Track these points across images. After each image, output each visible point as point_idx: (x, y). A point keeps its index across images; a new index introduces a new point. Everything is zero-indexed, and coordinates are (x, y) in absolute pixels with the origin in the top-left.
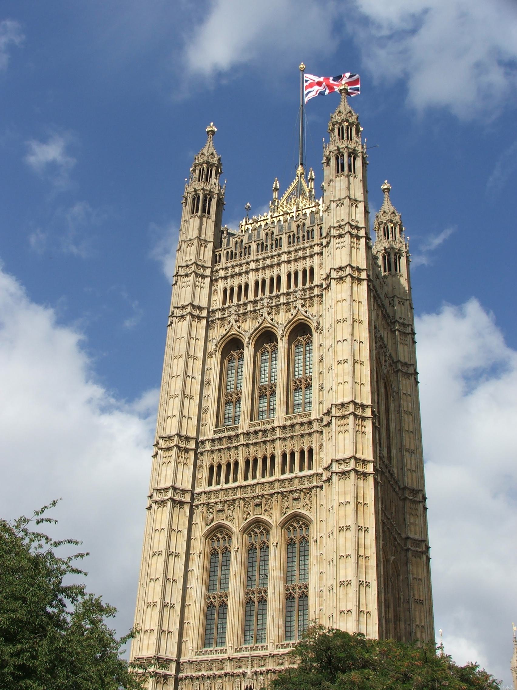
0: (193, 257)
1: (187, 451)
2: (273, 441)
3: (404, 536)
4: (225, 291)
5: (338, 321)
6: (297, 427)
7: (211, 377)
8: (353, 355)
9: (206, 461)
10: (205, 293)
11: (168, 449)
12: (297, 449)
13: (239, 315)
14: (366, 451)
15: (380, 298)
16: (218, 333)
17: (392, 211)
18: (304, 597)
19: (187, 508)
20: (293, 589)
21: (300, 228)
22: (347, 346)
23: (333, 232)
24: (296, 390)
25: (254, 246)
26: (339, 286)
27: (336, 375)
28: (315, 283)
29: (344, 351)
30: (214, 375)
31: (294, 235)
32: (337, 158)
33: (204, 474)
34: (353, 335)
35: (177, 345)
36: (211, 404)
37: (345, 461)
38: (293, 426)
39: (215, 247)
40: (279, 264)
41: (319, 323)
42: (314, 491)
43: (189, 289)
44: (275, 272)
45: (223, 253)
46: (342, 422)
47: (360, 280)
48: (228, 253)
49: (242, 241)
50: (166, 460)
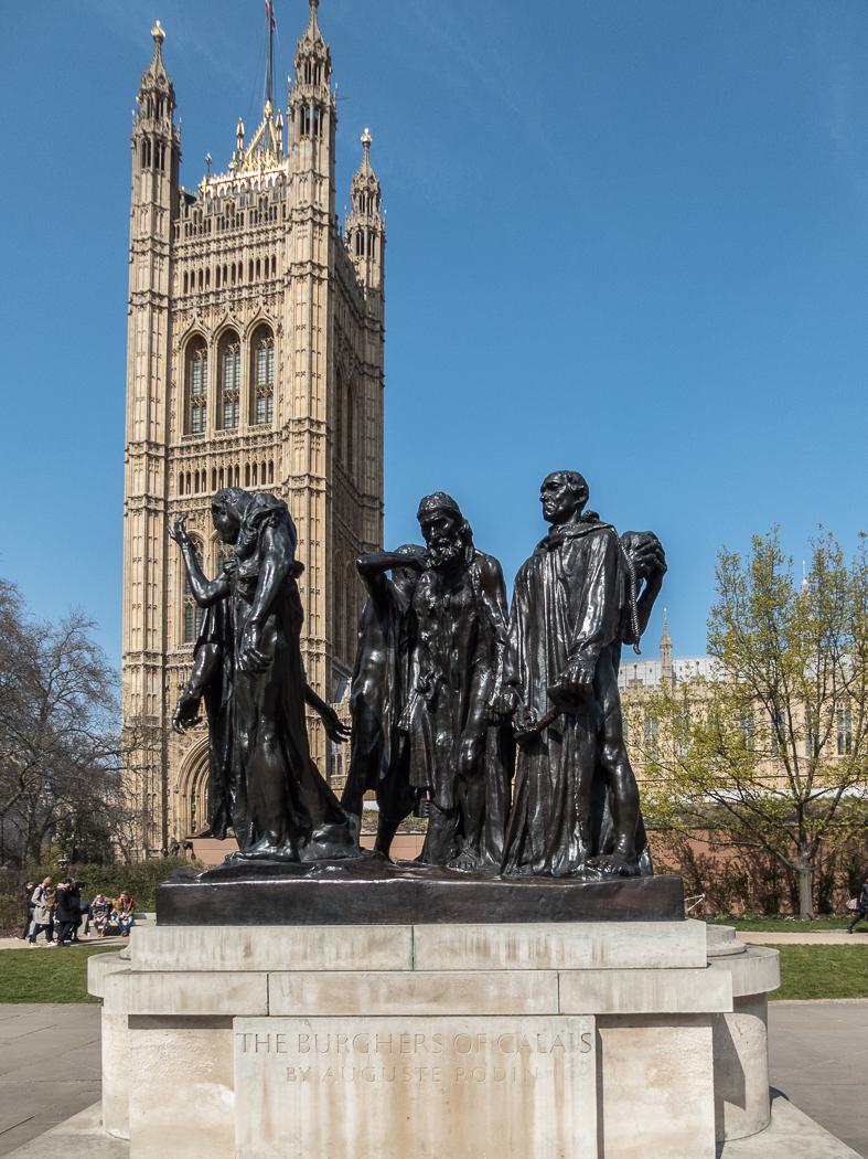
0: (149, 229)
1: (157, 458)
2: (237, 452)
3: (360, 541)
5: (298, 328)
6: (259, 439)
7: (177, 378)
8: (311, 368)
10: (165, 276)
11: (139, 456)
13: (201, 308)
14: (319, 469)
15: (348, 292)
16: (180, 327)
17: (370, 174)
19: (161, 516)
21: (263, 204)
22: (305, 358)
23: (296, 217)
24: (259, 398)
25: (214, 222)
26: (299, 285)
27: (294, 389)
28: (277, 278)
29: (302, 363)
30: (178, 376)
31: (256, 212)
33: (174, 483)
34: (311, 344)
35: (139, 339)
38: (255, 438)
41: (280, 326)
43: (147, 271)
45: (182, 226)
46: (298, 439)
47: (321, 280)
48: (187, 225)
49: (201, 212)
50: (137, 468)
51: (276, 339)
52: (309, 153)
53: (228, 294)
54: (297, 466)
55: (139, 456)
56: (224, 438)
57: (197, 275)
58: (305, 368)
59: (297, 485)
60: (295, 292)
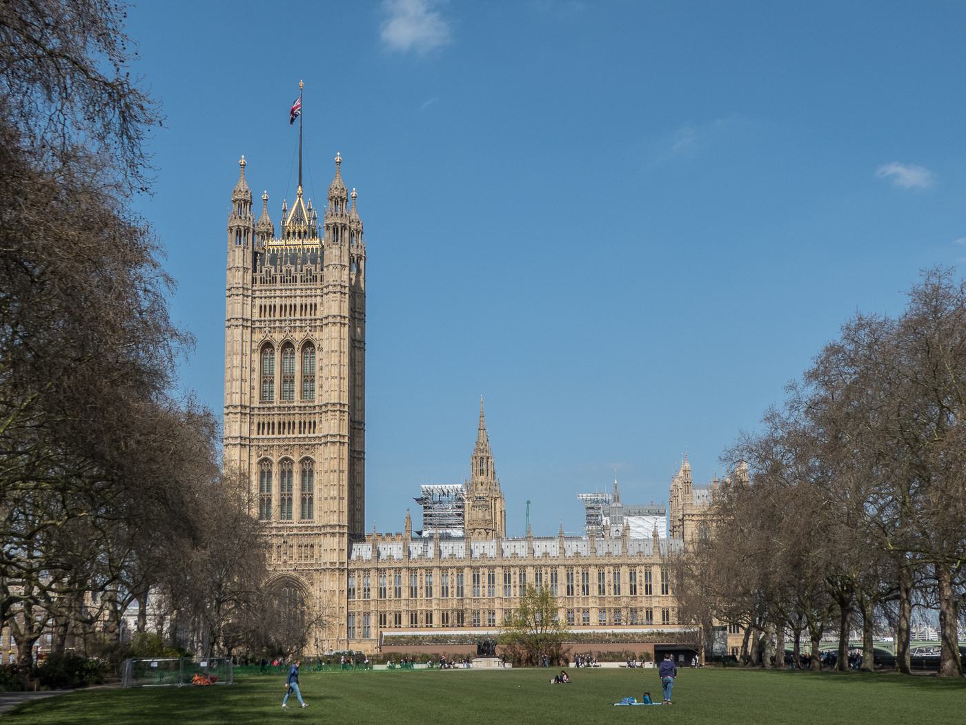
0: (240, 281)
1: (245, 414)
4: (261, 307)
8: (340, 375)
9: (256, 419)
11: (235, 414)
12: (307, 421)
16: (258, 337)
18: (311, 499)
20: (306, 495)
25: (278, 279)
26: (333, 328)
29: (335, 371)
30: (257, 366)
32: (334, 229)
33: (255, 427)
34: (340, 362)
35: (235, 345)
36: (256, 384)
37: (334, 436)
38: (305, 407)
39: (253, 272)
40: (295, 297)
42: (316, 446)
43: (240, 306)
44: (293, 301)
45: (258, 278)
46: (333, 413)
48: (261, 278)
51: (317, 352)
52: (338, 253)
53: (288, 322)
54: (332, 429)
55: (235, 414)
56: (285, 405)
57: (268, 308)
58: (337, 375)
59: (333, 440)
60: (330, 331)
